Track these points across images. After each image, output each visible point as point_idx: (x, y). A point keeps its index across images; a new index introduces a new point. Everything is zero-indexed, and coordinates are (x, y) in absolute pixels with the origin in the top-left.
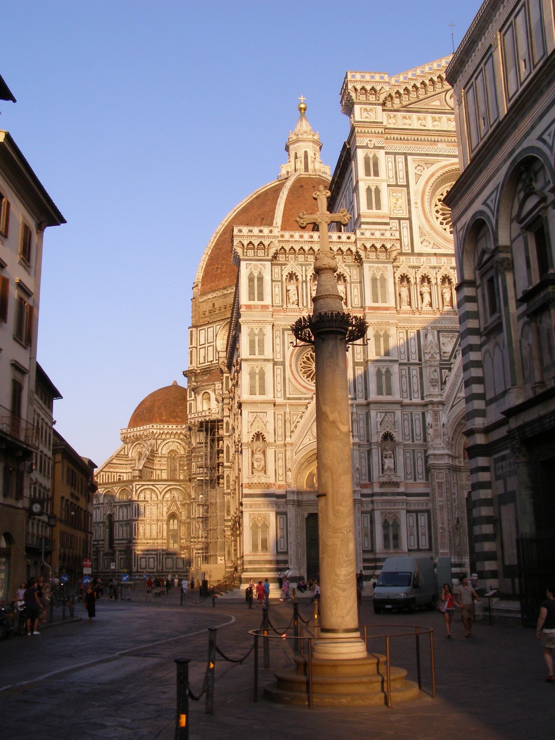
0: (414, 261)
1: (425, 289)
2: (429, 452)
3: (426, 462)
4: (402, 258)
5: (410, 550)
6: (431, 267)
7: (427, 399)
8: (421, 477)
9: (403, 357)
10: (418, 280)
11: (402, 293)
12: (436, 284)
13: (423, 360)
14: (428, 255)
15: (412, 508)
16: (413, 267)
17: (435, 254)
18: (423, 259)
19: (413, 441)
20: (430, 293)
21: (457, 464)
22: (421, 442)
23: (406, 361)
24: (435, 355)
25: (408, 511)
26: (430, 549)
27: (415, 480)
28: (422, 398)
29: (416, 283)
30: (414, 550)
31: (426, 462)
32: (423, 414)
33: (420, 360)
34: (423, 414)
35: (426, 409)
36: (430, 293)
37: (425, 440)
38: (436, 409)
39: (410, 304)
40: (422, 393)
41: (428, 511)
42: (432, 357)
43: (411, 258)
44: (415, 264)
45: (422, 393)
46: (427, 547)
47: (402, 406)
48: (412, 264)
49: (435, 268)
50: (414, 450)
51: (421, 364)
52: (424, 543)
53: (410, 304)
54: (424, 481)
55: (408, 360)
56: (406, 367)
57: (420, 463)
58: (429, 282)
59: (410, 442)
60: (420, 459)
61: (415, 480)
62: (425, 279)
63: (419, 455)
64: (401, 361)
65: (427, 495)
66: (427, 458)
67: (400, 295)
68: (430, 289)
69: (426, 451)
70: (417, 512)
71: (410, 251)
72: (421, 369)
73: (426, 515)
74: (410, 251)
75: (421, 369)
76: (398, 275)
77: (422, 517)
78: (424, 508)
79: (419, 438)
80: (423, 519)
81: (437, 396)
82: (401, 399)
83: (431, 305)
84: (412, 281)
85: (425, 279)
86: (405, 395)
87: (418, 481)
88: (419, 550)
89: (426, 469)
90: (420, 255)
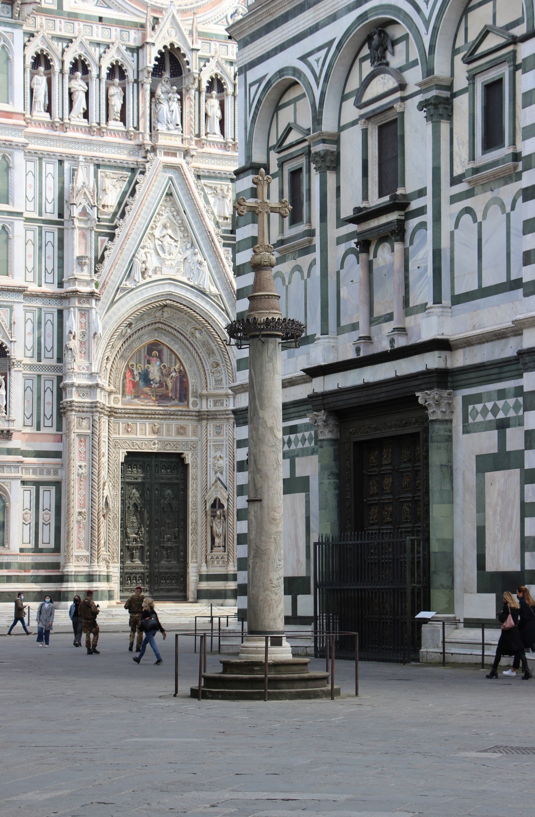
0: (62, 28)
1: (78, 85)
2: (67, 381)
3: (60, 397)
4: (41, 20)
5: (22, 550)
6: (92, 43)
7: (69, 288)
8: (48, 423)
9: (30, 206)
10: (68, 66)
11: (35, 87)
12: (99, 76)
13: (66, 216)
14: (88, 18)
15: (31, 476)
16: (60, 39)
17: (101, 19)
18: (79, 26)
19: (39, 360)
20: (87, 94)
21: (112, 405)
22: (54, 362)
23: (36, 216)
24: (88, 210)
25: (24, 483)
26: (57, 549)
27: (38, 429)
28: (61, 285)
29: (62, 72)
30: (29, 550)
31: (60, 397)
32: (60, 313)
33: (61, 215)
34: (60, 313)
35: (66, 303)
36: (87, 94)
37: (60, 359)
38: (86, 306)
39: (49, 109)
40: (61, 275)
41: (58, 484)
42: (84, 212)
43: (57, 21)
44: (63, 34)
45: (61, 275)
46: (52, 545)
47: (25, 296)
48: (58, 33)
49: (98, 44)
50: (39, 376)
51: (62, 223)
52: (47, 538)
53: (49, 109)
54: (53, 430)
55: (40, 214)
56: (35, 226)
57: (49, 398)
58: (86, 71)
59: (34, 361)
60: (49, 392)
61: (38, 429)
62: (80, 66)
63: (49, 384)
64: (26, 215)
65: (57, 454)
66: (61, 392)
67: (32, 91)
68: (87, 84)
69: (60, 379)
70: (37, 484)
71: (55, 7)
72: (61, 231)
73: (53, 489)
74: (55, 7)
75: (61, 231)
76: (31, 52)
77: (47, 494)
78: (51, 477)
79: (49, 355)
80: (48, 497)
81: (88, 283)
82: (24, 284)
83: (86, 115)
84: (57, 67)
85: (80, 66)
86: (30, 277)
87: (43, 430)
88: (37, 550)
89: (59, 409)
90: (73, 16)
